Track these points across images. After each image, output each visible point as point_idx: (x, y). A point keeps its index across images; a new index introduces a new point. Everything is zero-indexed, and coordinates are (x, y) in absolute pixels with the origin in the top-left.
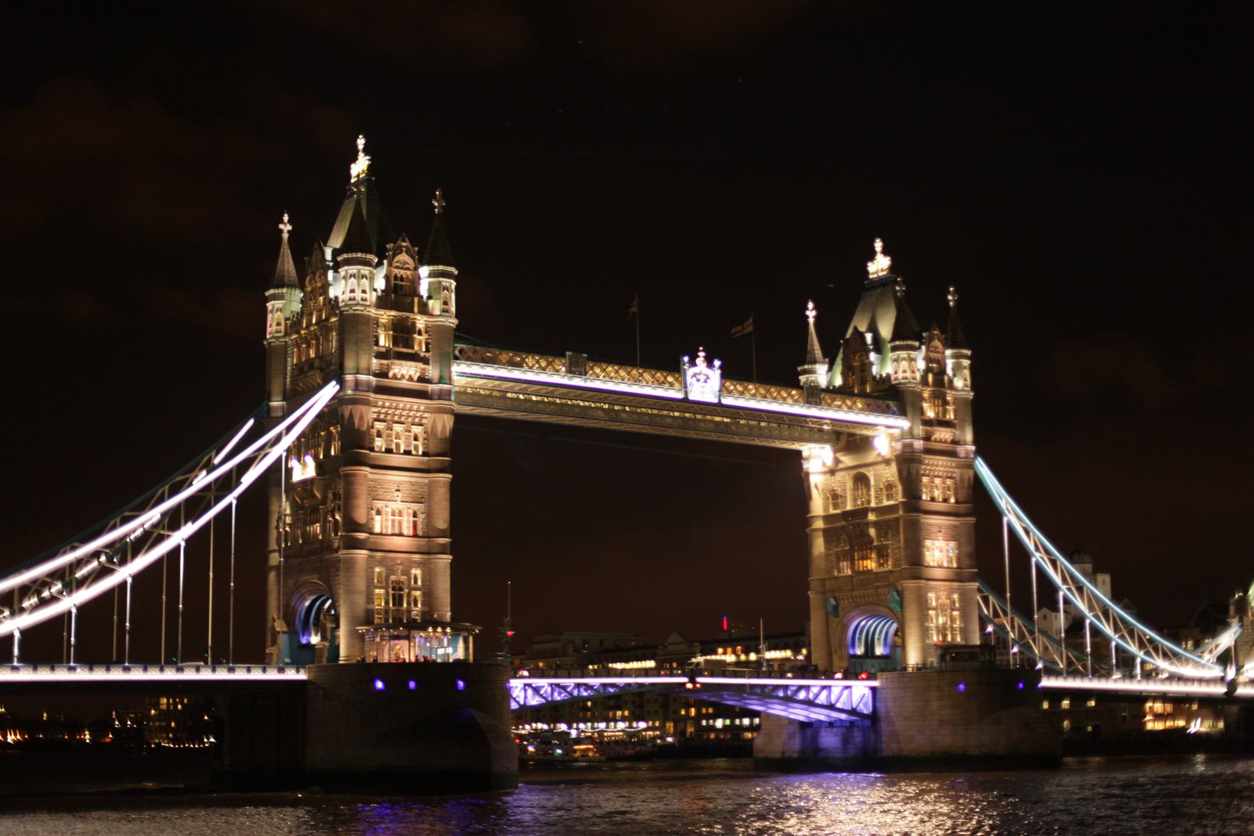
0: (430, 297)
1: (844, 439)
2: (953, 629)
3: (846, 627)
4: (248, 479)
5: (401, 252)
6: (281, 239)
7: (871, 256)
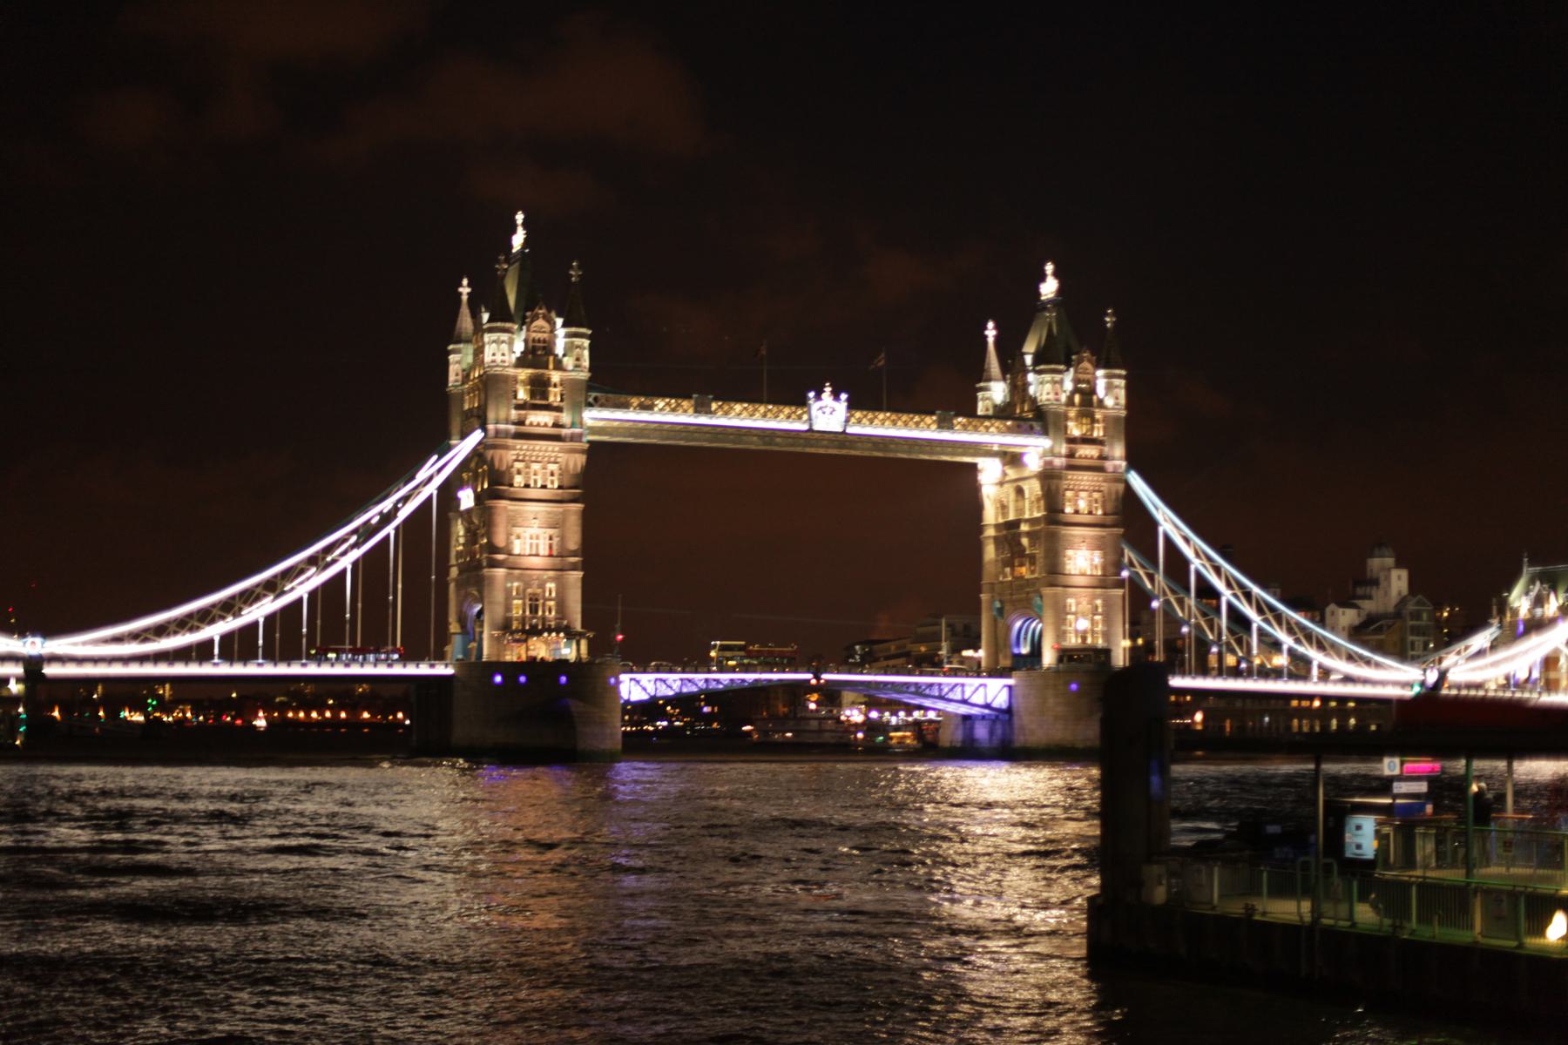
0: (564, 355)
1: (1008, 457)
2: (1093, 632)
3: (1009, 628)
4: (403, 514)
5: (538, 318)
7: (1043, 278)
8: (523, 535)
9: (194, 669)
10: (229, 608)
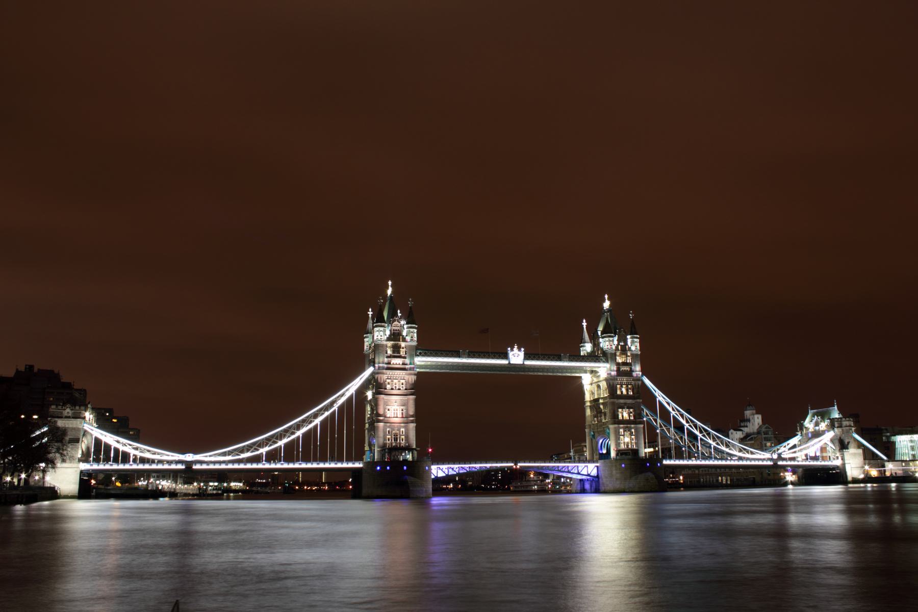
0: (406, 336)
3: (597, 443)
6: (369, 317)
7: (604, 301)
8: (390, 409)
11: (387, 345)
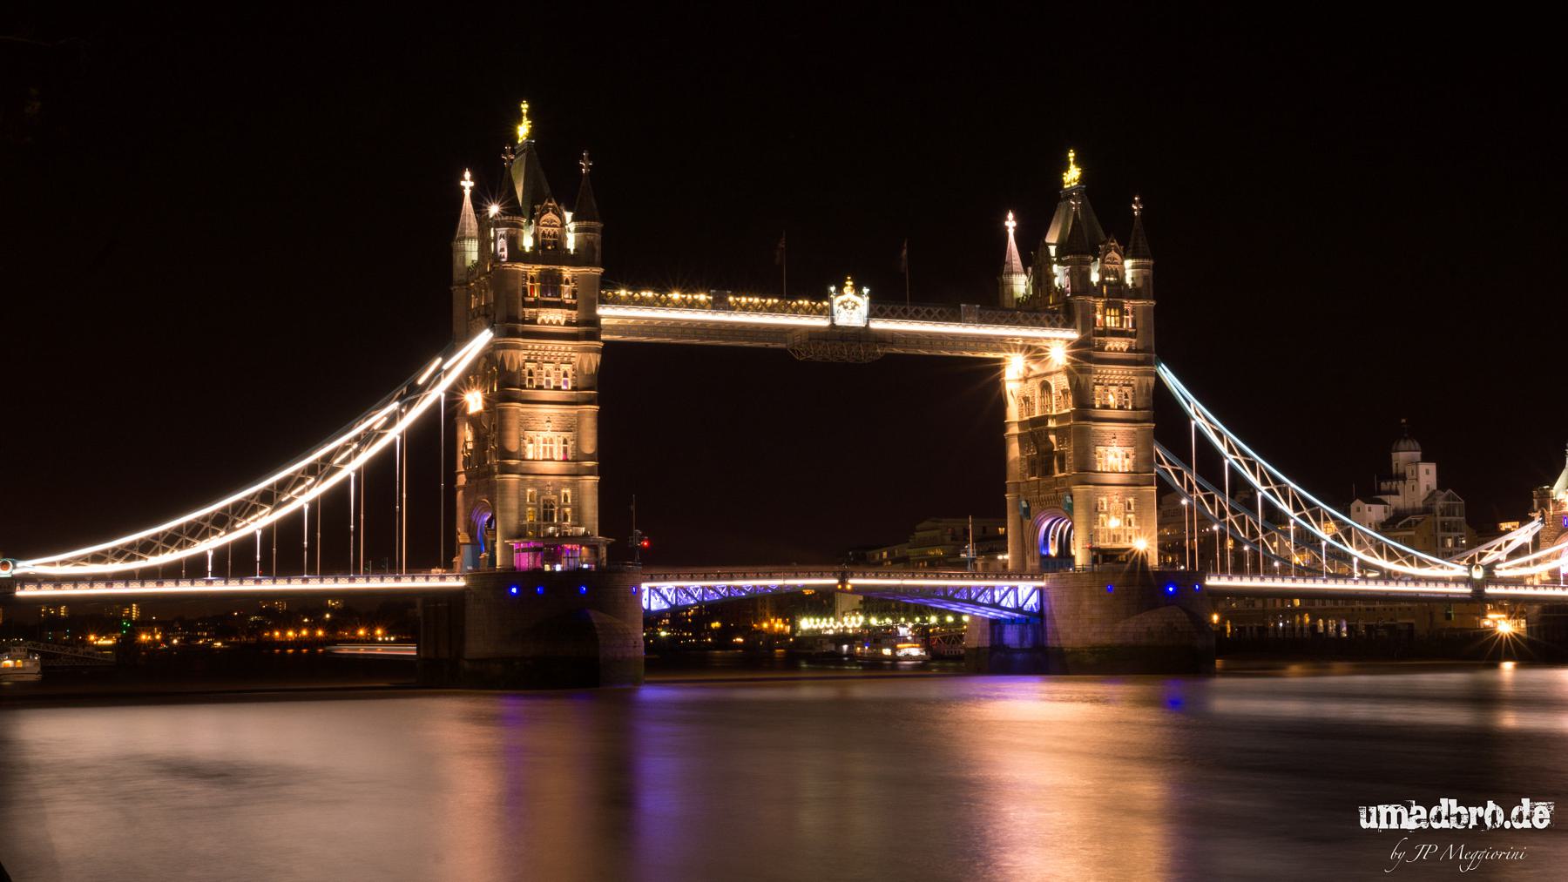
3: (1037, 528)
5: (548, 212)
6: (463, 195)
7: (1066, 167)
9: (185, 587)
10: (222, 521)
11: (526, 273)
